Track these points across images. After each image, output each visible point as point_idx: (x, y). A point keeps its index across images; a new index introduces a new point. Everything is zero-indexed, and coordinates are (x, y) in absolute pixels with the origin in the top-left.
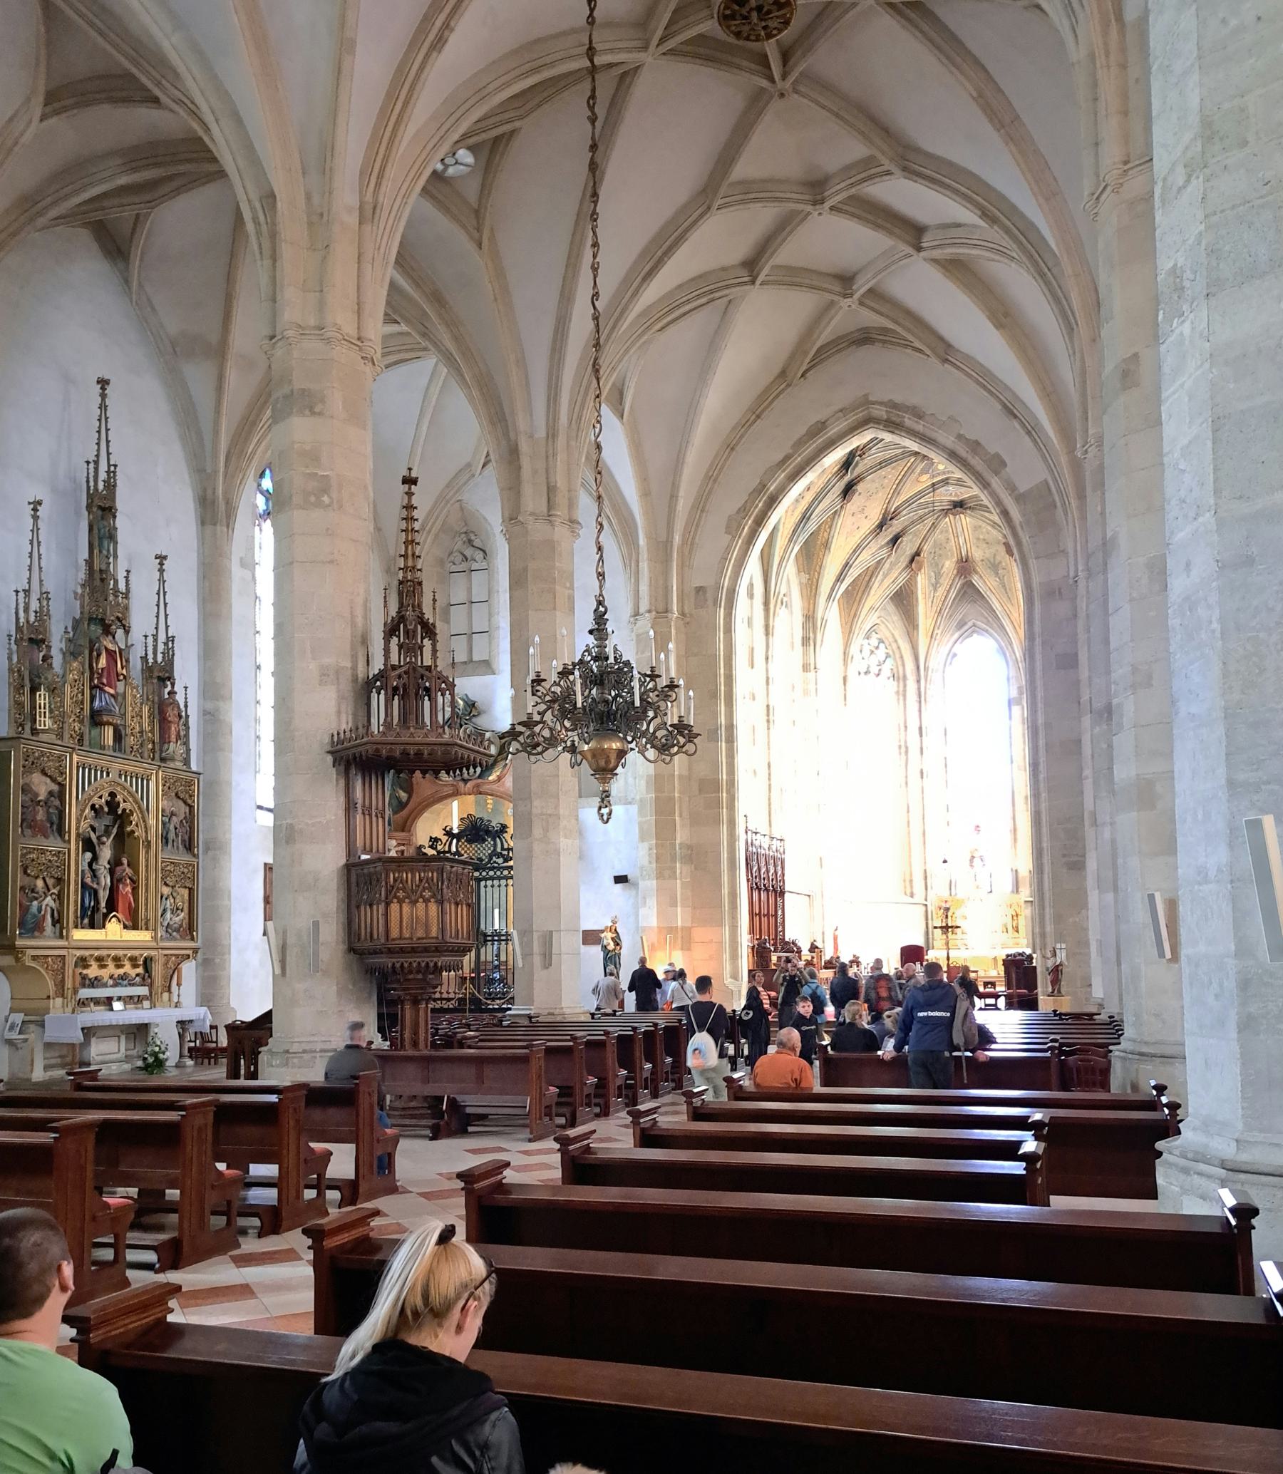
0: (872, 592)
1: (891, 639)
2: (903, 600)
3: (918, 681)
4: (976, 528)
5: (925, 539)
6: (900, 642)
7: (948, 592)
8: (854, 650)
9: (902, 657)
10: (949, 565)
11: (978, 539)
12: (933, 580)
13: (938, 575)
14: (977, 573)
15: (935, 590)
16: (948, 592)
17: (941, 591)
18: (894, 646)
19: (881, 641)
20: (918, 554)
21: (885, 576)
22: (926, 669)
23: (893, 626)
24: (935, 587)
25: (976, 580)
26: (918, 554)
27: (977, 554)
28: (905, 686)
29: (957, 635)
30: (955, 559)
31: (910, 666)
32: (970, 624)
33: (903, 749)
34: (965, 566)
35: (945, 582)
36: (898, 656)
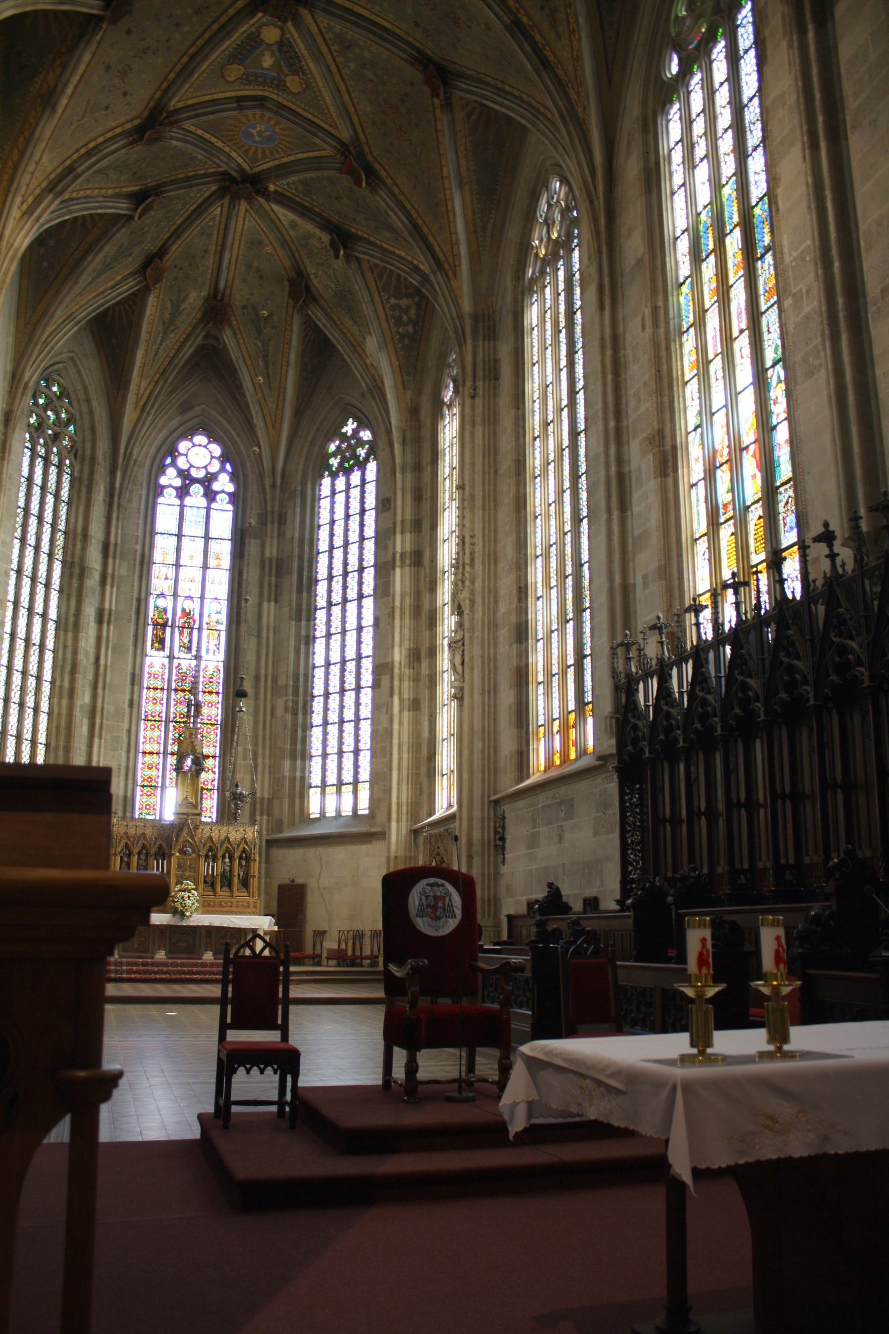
0: (82, 283)
1: (81, 395)
2: (112, 334)
3: (113, 473)
4: (255, 244)
5: (177, 234)
6: (95, 403)
7: (183, 344)
8: (31, 375)
9: (93, 428)
10: (195, 299)
11: (249, 266)
12: (167, 316)
13: (176, 309)
14: (231, 326)
15: (165, 334)
16: (183, 344)
17: (173, 338)
18: (85, 408)
19: (64, 393)
20: (161, 253)
21: (107, 267)
22: (128, 456)
23: (91, 372)
24: (168, 326)
25: (227, 337)
26: (161, 253)
27: (239, 295)
28: (92, 473)
29: (175, 422)
30: (204, 293)
31: (103, 447)
32: (198, 410)
33: (76, 571)
34: (216, 310)
35: (184, 324)
36: (87, 425)
